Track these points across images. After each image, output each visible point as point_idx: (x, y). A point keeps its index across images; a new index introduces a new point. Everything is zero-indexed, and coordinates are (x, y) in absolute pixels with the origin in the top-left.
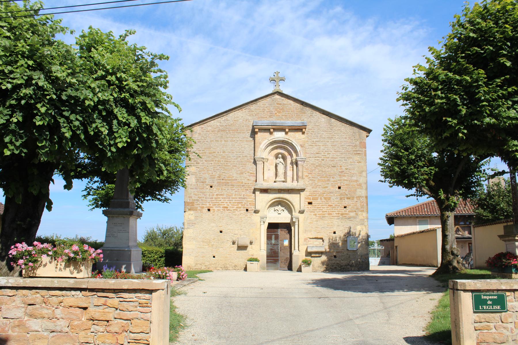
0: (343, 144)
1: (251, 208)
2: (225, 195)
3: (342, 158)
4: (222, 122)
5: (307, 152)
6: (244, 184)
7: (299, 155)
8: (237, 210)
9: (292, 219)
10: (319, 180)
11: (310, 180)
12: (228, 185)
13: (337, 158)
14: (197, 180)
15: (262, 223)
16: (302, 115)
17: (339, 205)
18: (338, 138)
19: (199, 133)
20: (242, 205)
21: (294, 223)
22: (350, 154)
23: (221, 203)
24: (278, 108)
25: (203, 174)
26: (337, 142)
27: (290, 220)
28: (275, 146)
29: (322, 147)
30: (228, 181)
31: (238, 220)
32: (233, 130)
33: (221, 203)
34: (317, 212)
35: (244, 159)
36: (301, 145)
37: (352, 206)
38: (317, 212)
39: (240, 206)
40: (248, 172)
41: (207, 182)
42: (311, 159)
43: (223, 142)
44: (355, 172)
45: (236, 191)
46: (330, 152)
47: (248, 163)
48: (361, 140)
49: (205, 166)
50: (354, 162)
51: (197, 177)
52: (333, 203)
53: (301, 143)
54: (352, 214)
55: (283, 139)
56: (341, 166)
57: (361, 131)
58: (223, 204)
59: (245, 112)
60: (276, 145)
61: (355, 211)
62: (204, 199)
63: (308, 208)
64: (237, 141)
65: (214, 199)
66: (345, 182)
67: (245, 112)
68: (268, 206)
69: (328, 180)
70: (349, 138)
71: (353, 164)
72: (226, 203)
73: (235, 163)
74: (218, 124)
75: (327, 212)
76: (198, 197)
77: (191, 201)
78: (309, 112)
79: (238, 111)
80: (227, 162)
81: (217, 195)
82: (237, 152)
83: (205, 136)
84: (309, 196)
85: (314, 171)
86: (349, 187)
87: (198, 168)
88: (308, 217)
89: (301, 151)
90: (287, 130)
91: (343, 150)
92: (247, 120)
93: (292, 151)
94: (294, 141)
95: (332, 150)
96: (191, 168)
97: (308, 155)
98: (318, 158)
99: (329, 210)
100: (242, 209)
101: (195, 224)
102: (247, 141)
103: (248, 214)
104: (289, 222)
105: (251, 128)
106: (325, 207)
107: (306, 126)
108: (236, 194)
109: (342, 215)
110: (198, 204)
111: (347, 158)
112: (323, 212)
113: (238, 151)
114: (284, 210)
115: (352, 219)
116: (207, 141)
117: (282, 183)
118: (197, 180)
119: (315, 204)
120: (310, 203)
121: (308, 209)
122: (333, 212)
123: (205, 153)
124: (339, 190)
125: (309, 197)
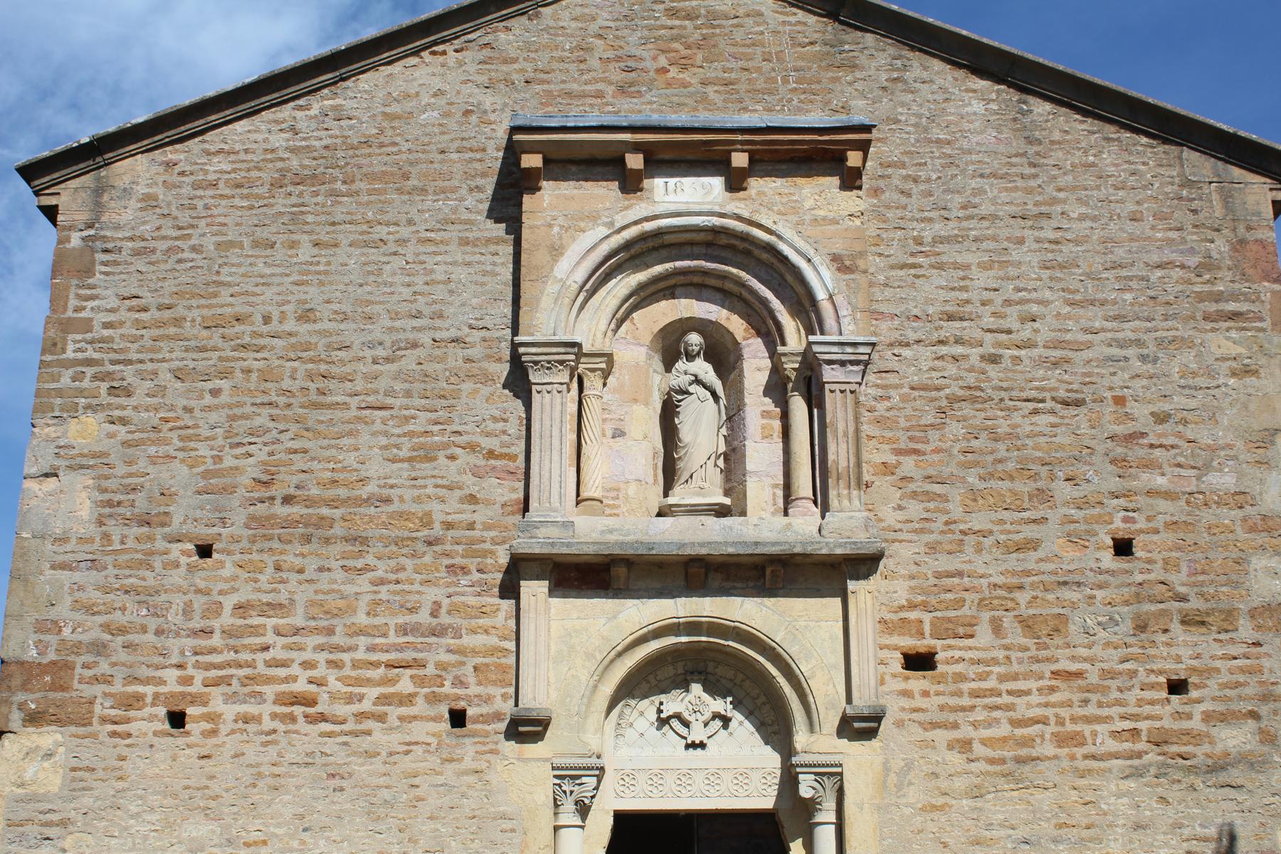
0: (1120, 253)
1: (488, 699)
2: (300, 610)
3: (1122, 345)
4: (301, 125)
5: (882, 308)
6: (437, 530)
7: (830, 322)
8: (381, 718)
9: (789, 779)
10: (974, 494)
11: (914, 495)
12: (327, 541)
13: (1089, 345)
14: (108, 507)
15: (569, 816)
16: (837, 80)
17: (1132, 674)
18: (1082, 218)
19: (147, 197)
20: (419, 681)
21: (808, 808)
22: (1175, 316)
23: (269, 664)
24: (674, 39)
25: (153, 460)
26: (1076, 242)
27: (773, 792)
28: (658, 269)
29: (982, 279)
30: (325, 511)
31: (385, 794)
32: (371, 177)
33: (269, 664)
34: (975, 725)
35: (441, 360)
36: (835, 258)
37: (1225, 678)
38: (975, 725)
39: (405, 685)
40: (472, 447)
41: (177, 520)
42: (906, 352)
43: (305, 252)
44: (1224, 437)
45: (382, 582)
46: (1035, 308)
47: (467, 386)
48: (1241, 230)
49: (172, 408)
50: (1211, 374)
51: (105, 484)
52: (1091, 660)
53: (838, 247)
54: (1234, 738)
55: (716, 221)
56: (1120, 401)
57: (1237, 172)
58: (282, 672)
59: (461, 64)
60: (669, 266)
61: (1254, 715)
62: (150, 637)
63: (906, 694)
64: (402, 242)
65: (216, 640)
66: (1162, 505)
67: (461, 64)
68: (609, 688)
69: (1044, 496)
70: (1158, 216)
71: (1202, 381)
72: (307, 665)
73: (382, 384)
74: (279, 140)
75: (1044, 721)
76: (106, 627)
77: (52, 656)
78: (883, 59)
79: (413, 60)
80: (321, 384)
81: (241, 608)
82: (395, 316)
83: (184, 217)
84: (912, 606)
85: (933, 435)
86: (1190, 538)
87: (123, 421)
88: (909, 766)
89: (839, 299)
90: (740, 160)
91: (1128, 296)
92: (467, 113)
93: (776, 304)
94: (788, 233)
95: (1047, 294)
96: (73, 426)
97: (884, 326)
98: (959, 350)
99: (1065, 713)
100: (420, 707)
101: (64, 823)
102: (464, 242)
103: (468, 749)
104: (767, 803)
105: (495, 158)
106: (1033, 685)
107: (867, 129)
108: (377, 603)
109: (1159, 741)
110: (96, 679)
111: (1160, 342)
112: (1016, 723)
113: (404, 308)
114: (726, 721)
115: (1235, 775)
116: (194, 249)
117: (711, 521)
118: (109, 503)
119: (959, 668)
120: (919, 662)
121: (906, 703)
122: (1088, 720)
123: (178, 322)
124: (1122, 563)
125: (913, 615)
